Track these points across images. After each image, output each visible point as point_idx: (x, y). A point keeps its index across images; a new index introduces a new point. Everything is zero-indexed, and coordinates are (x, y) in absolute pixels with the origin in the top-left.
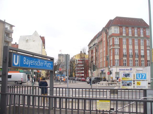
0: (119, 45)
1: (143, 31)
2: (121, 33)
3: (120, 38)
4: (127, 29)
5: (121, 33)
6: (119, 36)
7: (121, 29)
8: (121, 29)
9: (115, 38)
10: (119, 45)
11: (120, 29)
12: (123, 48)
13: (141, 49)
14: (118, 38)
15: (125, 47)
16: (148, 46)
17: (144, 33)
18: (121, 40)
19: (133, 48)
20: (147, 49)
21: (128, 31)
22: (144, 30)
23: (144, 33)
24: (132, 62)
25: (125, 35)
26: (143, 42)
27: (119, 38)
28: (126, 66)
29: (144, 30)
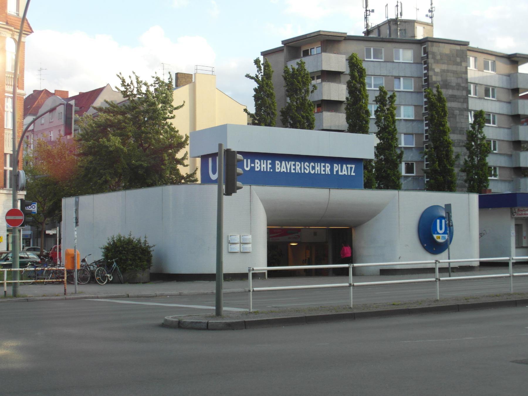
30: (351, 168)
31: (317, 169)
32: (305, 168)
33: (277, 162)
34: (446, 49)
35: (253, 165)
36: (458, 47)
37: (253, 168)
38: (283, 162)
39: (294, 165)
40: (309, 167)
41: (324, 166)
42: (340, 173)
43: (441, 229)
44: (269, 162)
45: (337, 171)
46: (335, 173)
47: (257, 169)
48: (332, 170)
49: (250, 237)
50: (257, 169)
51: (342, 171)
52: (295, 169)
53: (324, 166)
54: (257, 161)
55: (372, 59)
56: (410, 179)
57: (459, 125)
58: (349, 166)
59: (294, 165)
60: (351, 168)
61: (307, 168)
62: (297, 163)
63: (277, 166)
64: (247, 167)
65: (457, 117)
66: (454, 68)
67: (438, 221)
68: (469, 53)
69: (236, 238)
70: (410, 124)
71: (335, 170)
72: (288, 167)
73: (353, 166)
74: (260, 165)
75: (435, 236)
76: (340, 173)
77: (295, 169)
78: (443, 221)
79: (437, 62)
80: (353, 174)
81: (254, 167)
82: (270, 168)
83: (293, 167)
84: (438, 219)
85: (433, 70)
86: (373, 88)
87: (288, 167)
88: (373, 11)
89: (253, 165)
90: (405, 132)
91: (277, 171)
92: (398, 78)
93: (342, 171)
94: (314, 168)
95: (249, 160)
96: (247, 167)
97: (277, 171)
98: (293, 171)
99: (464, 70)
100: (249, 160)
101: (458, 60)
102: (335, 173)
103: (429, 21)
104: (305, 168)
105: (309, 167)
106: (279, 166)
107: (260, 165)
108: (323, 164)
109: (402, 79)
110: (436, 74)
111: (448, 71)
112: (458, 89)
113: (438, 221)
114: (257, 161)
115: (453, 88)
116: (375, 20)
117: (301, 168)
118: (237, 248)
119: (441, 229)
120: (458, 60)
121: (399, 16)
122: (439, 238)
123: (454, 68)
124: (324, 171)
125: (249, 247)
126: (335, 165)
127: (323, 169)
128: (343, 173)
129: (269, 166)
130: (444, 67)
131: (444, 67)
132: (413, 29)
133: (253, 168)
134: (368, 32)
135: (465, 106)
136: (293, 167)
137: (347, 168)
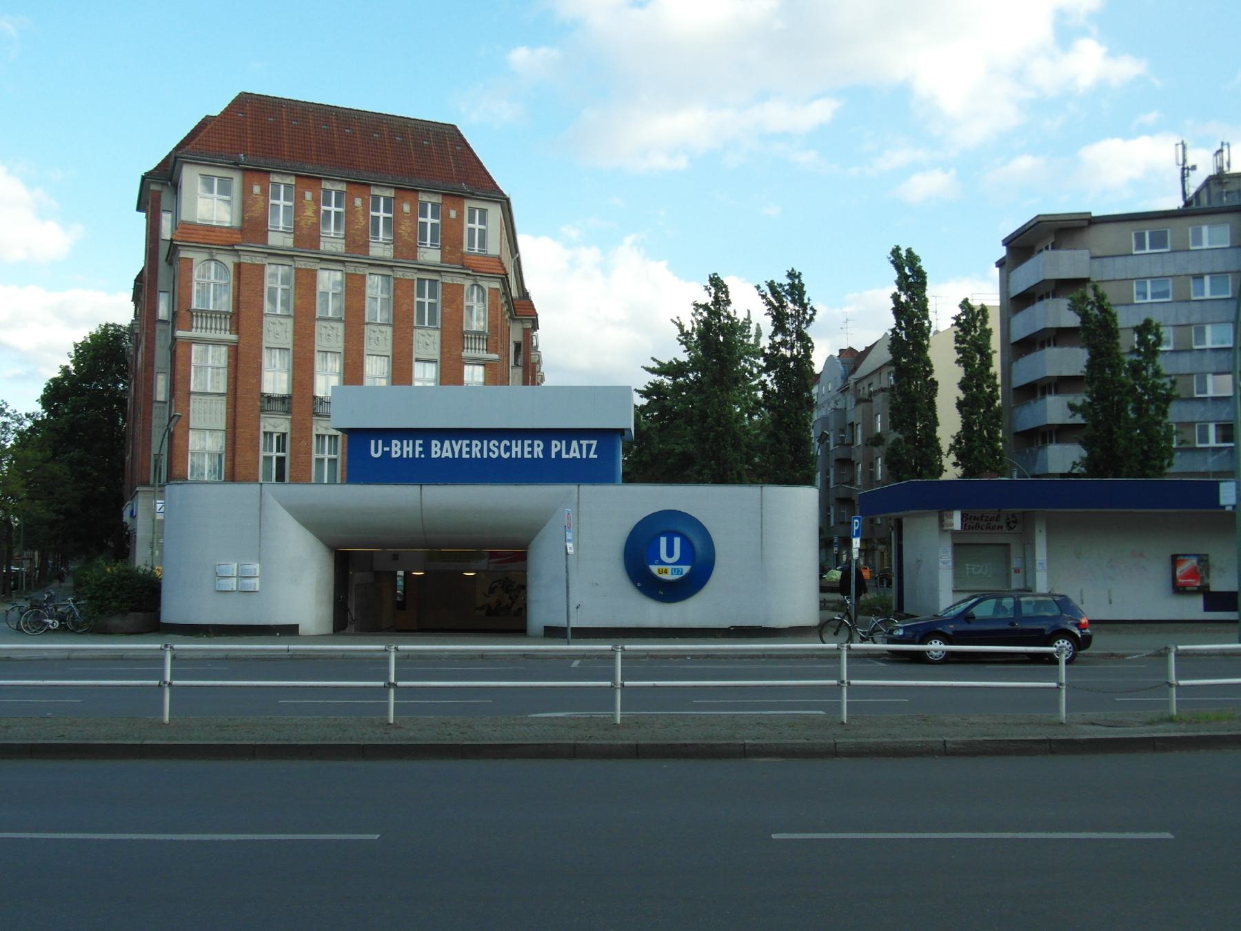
1: (445, 217)
2: (253, 228)
3: (246, 259)
5: (253, 228)
6: (231, 248)
7: (257, 189)
8: (257, 189)
9: (198, 257)
10: (235, 319)
11: (246, 190)
12: (268, 339)
13: (415, 356)
14: (229, 261)
15: (277, 332)
17: (449, 238)
18: (246, 284)
19: (346, 341)
20: (465, 354)
21: (317, 212)
22: (453, 214)
23: (449, 238)
24: (339, 456)
25: (289, 241)
26: (439, 301)
27: (238, 266)
28: (287, 479)
29: (453, 214)
30: (589, 446)
31: (514, 449)
32: (489, 450)
33: (434, 442)
35: (387, 449)
37: (387, 455)
38: (447, 443)
39: (469, 446)
40: (498, 447)
41: (531, 446)
42: (564, 456)
43: (670, 553)
44: (418, 442)
45: (559, 453)
46: (553, 456)
47: (394, 456)
48: (547, 450)
49: (257, 566)
50: (394, 456)
51: (568, 452)
52: (469, 453)
53: (531, 446)
54: (394, 442)
55: (1148, 250)
56: (1225, 452)
58: (584, 443)
59: (469, 446)
60: (589, 446)
61: (496, 449)
62: (474, 442)
63: (434, 449)
64: (376, 451)
67: (663, 541)
69: (233, 568)
70: (1223, 356)
71: (554, 451)
72: (457, 450)
73: (594, 443)
74: (402, 449)
75: (654, 569)
76: (564, 456)
77: (469, 453)
78: (677, 541)
80: (592, 456)
81: (390, 452)
82: (420, 453)
83: (465, 449)
84: (663, 534)
86: (1149, 300)
87: (457, 450)
88: (1194, 168)
89: (387, 449)
90: (1214, 369)
91: (433, 456)
92: (1199, 277)
93: (568, 452)
94: (508, 449)
95: (380, 442)
96: (376, 451)
97: (433, 456)
98: (465, 456)
100: (380, 442)
102: (553, 456)
104: (489, 450)
105: (498, 447)
106: (438, 449)
107: (402, 449)
108: (527, 442)
109: (1207, 279)
113: (663, 541)
114: (394, 442)
116: (1195, 182)
117: (481, 451)
118: (232, 584)
119: (670, 553)
121: (1225, 168)
122: (666, 572)
124: (531, 453)
125: (255, 584)
126: (554, 442)
127: (527, 449)
128: (572, 455)
129: (418, 449)
133: (387, 455)
134: (1187, 203)
136: (465, 449)
137: (580, 446)
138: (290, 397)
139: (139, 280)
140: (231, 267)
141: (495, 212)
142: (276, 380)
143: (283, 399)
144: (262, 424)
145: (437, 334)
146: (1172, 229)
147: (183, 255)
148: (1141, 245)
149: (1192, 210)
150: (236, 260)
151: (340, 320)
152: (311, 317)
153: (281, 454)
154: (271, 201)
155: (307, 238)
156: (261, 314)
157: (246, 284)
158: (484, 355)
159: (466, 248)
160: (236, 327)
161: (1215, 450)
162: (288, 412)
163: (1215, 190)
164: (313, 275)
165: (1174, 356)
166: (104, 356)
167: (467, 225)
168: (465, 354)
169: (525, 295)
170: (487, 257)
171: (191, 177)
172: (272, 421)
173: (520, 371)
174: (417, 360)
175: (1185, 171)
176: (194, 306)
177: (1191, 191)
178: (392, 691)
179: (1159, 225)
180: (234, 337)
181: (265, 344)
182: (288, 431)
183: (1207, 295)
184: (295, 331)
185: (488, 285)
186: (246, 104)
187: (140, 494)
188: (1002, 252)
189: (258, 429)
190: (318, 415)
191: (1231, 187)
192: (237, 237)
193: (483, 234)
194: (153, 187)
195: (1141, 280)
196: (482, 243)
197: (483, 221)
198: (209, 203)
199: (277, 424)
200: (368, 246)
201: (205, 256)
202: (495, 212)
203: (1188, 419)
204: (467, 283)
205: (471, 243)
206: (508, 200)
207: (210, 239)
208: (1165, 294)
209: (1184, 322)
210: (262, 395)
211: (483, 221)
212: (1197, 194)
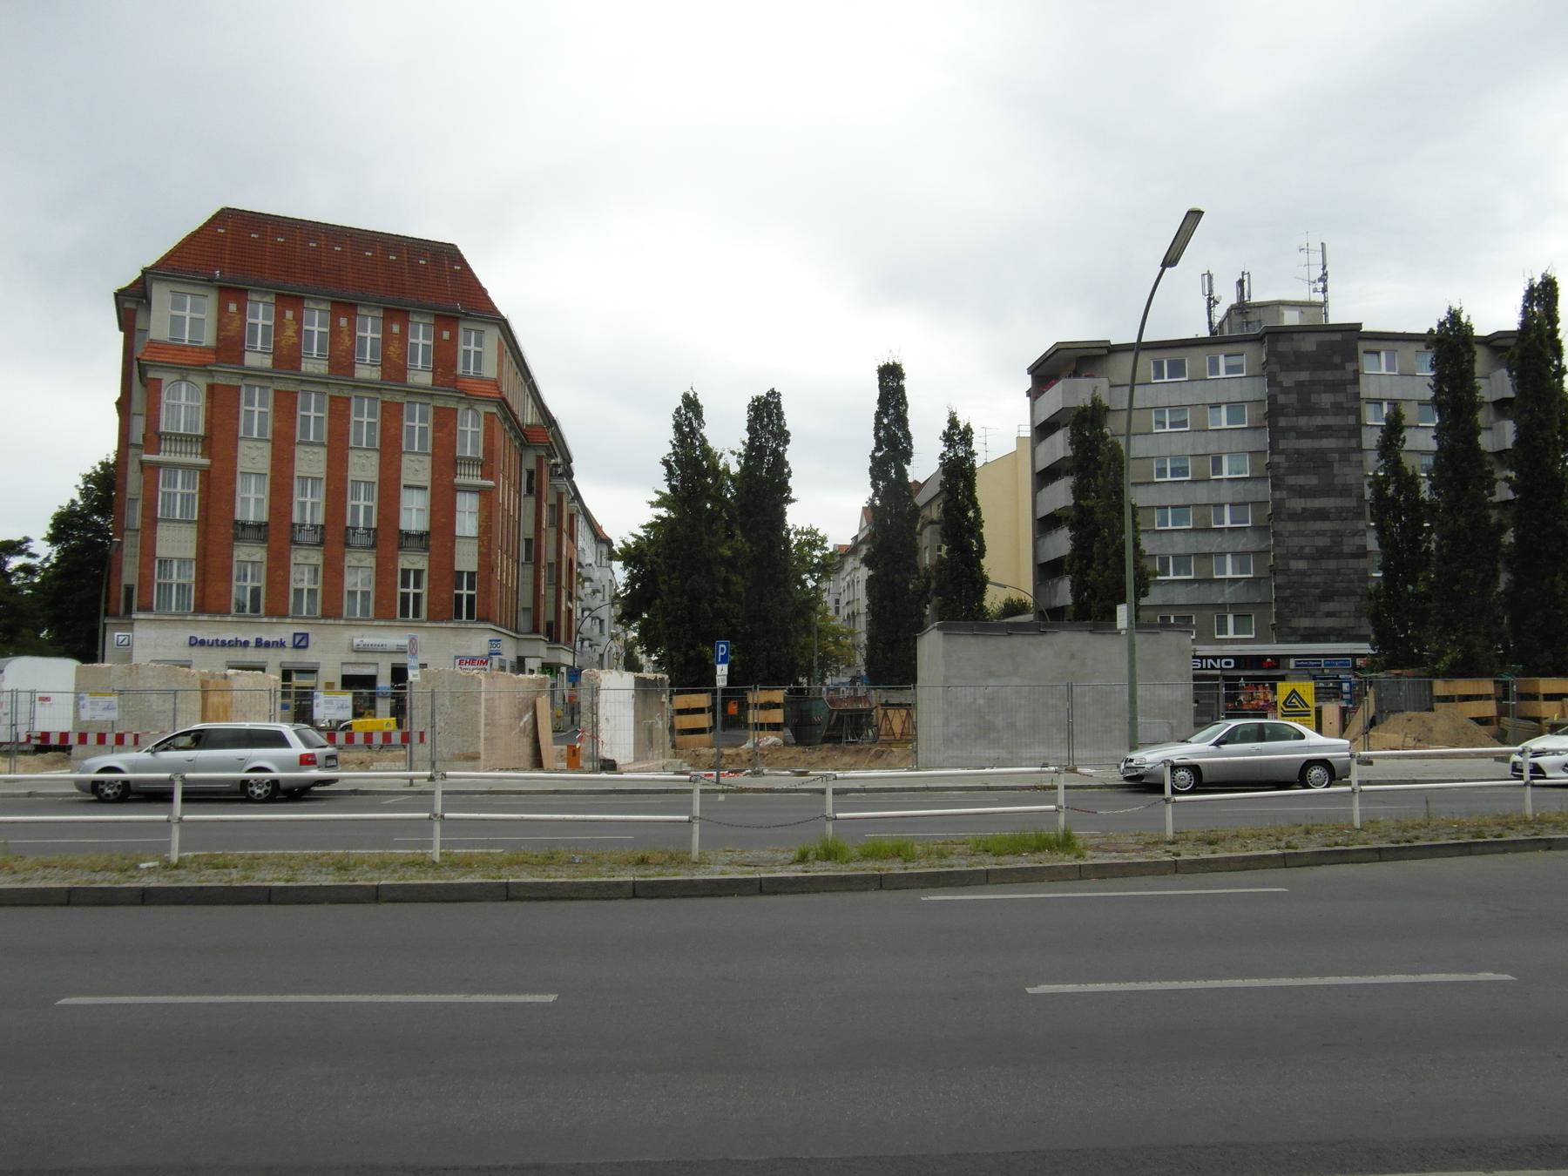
0: (207, 443)
1: (438, 337)
2: (230, 347)
3: (219, 380)
4: (289, 314)
5: (230, 347)
6: (202, 368)
7: (233, 307)
8: (233, 307)
9: (167, 378)
10: (207, 443)
11: (222, 309)
12: (243, 464)
13: (403, 482)
14: (201, 382)
15: (254, 457)
16: (471, 462)
17: (444, 360)
18: (222, 404)
19: (329, 466)
20: (458, 480)
21: (299, 332)
22: (446, 335)
23: (444, 360)
24: (319, 586)
25: (267, 362)
26: (429, 425)
27: (212, 389)
28: (262, 611)
29: (446, 335)
34: (1309, 344)
36: (1338, 337)
55: (1166, 379)
57: (1338, 481)
65: (1336, 466)
66: (1328, 375)
68: (1362, 346)
70: (1240, 486)
79: (1287, 368)
85: (1280, 384)
86: (1168, 429)
92: (1217, 406)
99: (1351, 377)
101: (1337, 359)
103: (1319, 298)
110: (1286, 391)
111: (1312, 383)
112: (1336, 415)
115: (1323, 412)
116: (1220, 312)
120: (1337, 359)
123: (1328, 375)
130: (1304, 376)
131: (1304, 376)
132: (1279, 316)
135: (1353, 443)
138: (267, 524)
139: (119, 404)
140: (204, 388)
141: (492, 336)
142: (252, 504)
143: (259, 526)
144: (235, 553)
145: (428, 461)
146: (1191, 359)
147: (151, 375)
148: (1159, 374)
149: (1216, 340)
150: (210, 381)
151: (322, 445)
152: (291, 442)
153: (256, 584)
154: (250, 320)
155: (287, 359)
156: (236, 438)
157: (222, 404)
158: (479, 481)
159: (460, 370)
160: (208, 451)
161: (1231, 580)
162: (265, 540)
163: (1237, 320)
164: (293, 396)
165: (1193, 486)
166: (105, 487)
167: (462, 347)
168: (458, 480)
169: (549, 421)
170: (482, 380)
171: (161, 295)
172: (248, 550)
173: (532, 500)
174: (425, 488)
175: (1212, 302)
176: (163, 428)
177: (1217, 321)
178: (437, 826)
179: (1176, 354)
180: (206, 462)
181: (239, 469)
182: (321, 562)
183: (1224, 425)
184: (273, 455)
185: (483, 409)
186: (227, 217)
187: (136, 624)
188: (1027, 382)
189: (231, 557)
190: (296, 543)
191: (1251, 318)
192: (211, 358)
193: (478, 355)
194: (127, 305)
195: (1160, 410)
196: (478, 365)
197: (479, 343)
198: (186, 317)
199: (250, 555)
200: (353, 368)
201: (177, 377)
202: (492, 336)
203: (1206, 550)
204: (461, 407)
205: (467, 365)
206: (505, 321)
207: (185, 361)
208: (1184, 423)
209: (1201, 452)
210: (236, 522)
211: (479, 343)
212: (1221, 324)
